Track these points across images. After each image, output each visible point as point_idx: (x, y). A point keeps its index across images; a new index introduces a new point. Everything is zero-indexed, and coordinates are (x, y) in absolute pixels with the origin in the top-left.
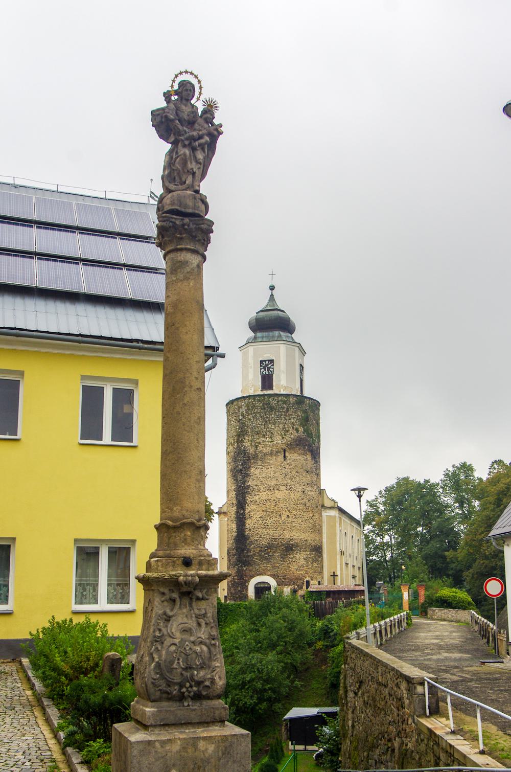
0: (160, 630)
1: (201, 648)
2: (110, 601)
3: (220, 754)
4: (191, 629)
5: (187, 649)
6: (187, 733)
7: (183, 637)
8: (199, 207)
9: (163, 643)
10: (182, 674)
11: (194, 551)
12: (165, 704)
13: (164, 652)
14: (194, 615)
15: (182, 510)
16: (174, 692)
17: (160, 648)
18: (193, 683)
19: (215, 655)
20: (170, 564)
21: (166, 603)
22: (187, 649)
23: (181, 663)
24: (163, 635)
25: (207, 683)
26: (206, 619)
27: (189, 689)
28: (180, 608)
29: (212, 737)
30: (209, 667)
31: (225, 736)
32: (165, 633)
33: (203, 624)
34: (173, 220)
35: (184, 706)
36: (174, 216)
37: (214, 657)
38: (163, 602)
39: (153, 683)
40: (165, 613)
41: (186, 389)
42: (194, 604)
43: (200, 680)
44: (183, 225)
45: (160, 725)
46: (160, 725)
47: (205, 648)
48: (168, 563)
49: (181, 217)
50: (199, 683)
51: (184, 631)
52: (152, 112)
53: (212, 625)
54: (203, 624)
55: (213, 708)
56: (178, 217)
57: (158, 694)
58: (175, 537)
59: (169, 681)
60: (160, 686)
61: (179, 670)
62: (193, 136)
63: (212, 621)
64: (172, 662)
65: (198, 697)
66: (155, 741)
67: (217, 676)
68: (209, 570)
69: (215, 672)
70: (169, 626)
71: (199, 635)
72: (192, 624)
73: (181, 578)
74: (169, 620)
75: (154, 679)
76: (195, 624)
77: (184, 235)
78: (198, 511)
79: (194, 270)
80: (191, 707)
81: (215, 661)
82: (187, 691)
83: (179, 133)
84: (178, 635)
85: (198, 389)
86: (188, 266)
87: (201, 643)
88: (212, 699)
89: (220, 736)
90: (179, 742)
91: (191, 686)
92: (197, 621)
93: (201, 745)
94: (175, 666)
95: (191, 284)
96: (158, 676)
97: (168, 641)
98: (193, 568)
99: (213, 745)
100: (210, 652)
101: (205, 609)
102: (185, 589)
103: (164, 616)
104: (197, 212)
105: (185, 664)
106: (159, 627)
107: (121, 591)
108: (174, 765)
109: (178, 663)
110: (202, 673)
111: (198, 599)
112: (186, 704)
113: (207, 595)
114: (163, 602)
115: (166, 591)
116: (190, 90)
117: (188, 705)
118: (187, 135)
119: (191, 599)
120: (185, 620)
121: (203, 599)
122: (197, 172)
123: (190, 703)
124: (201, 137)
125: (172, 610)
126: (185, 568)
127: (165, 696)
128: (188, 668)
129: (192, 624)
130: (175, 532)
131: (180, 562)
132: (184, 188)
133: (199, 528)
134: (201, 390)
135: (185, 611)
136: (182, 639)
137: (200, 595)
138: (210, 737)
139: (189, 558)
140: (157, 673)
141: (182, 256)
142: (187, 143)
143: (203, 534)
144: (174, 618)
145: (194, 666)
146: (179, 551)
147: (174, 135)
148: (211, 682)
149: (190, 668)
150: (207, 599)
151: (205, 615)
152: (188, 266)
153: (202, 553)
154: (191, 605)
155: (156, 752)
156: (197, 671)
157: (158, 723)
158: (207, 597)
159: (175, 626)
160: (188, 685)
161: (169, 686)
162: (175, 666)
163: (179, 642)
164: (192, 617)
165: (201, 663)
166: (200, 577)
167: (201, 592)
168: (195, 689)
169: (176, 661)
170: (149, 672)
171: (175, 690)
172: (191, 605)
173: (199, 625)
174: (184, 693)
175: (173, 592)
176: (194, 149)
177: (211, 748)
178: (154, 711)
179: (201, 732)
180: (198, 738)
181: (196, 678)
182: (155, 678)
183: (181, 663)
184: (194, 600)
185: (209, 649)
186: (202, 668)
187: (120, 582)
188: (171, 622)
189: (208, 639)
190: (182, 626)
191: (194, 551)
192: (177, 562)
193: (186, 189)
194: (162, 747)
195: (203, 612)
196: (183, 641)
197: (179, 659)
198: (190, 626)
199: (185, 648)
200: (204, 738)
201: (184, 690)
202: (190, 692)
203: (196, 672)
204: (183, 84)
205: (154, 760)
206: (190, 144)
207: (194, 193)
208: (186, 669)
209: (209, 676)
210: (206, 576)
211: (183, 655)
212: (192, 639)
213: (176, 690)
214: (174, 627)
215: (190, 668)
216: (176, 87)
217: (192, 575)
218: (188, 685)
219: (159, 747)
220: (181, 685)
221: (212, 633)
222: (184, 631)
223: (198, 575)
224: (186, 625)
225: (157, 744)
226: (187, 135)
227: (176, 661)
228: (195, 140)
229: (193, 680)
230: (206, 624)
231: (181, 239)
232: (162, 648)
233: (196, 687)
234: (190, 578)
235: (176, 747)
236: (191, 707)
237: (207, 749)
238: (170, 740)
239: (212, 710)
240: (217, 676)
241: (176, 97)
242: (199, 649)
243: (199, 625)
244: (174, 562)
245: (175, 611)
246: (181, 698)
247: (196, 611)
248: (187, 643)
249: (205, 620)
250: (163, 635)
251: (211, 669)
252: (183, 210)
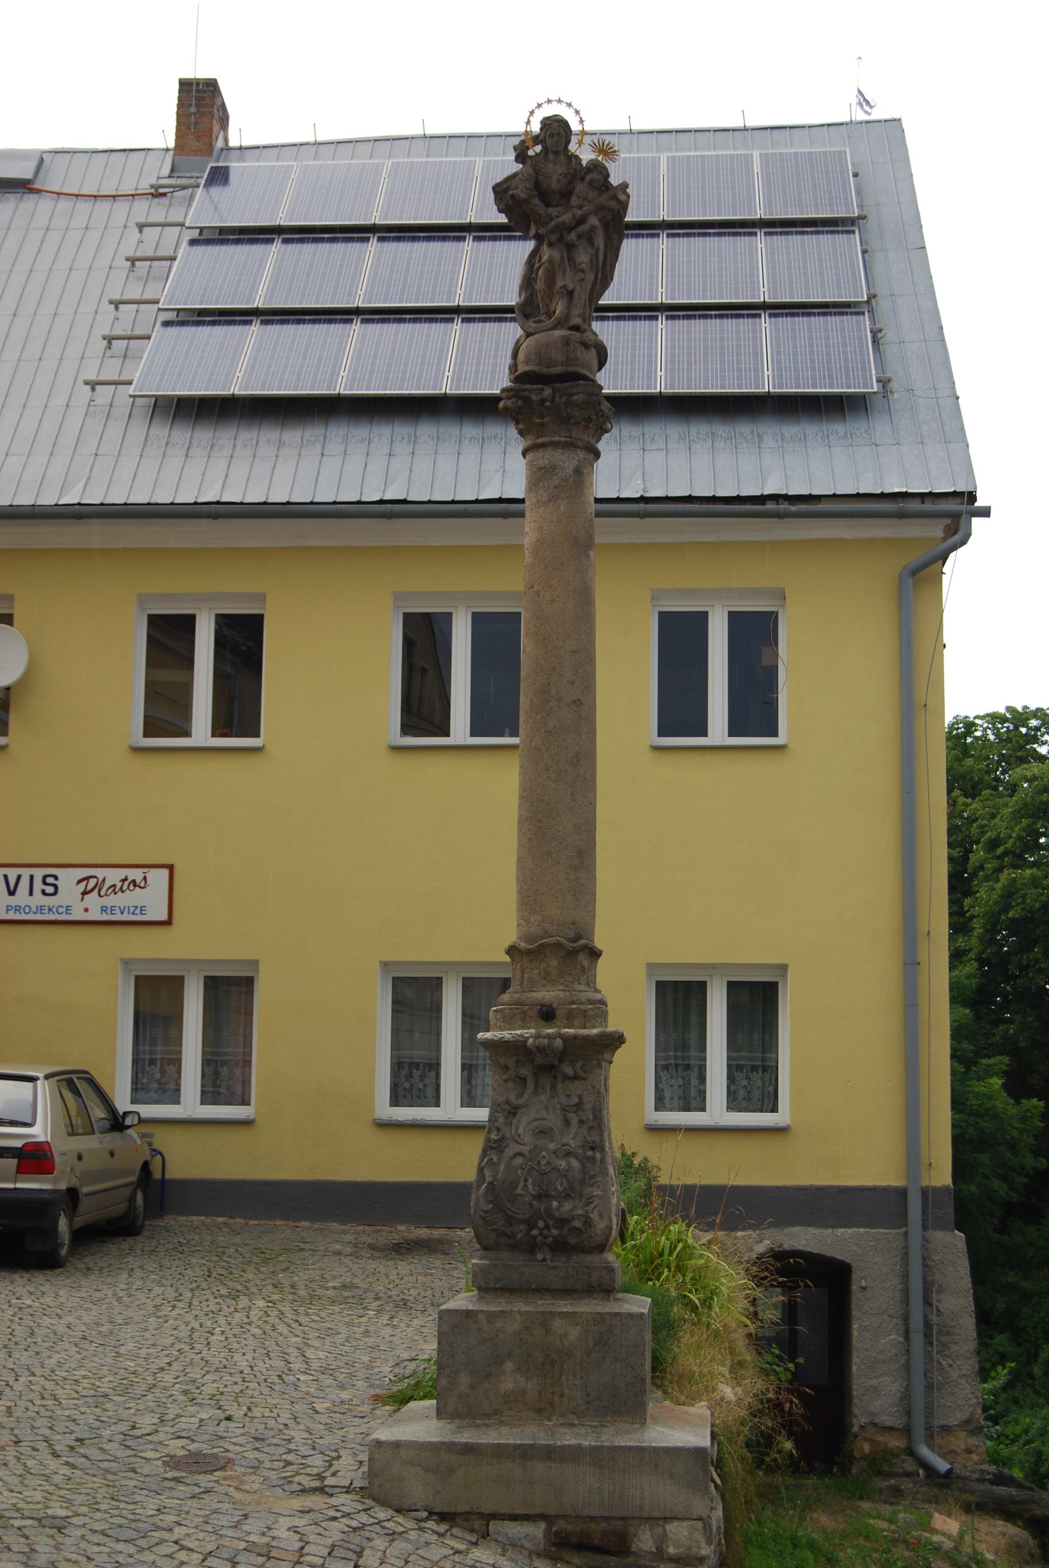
0: (498, 1129)
1: (568, 1164)
2: (734, 1103)
3: (591, 1342)
4: (551, 1129)
5: (543, 1163)
6: (542, 1305)
7: (538, 1143)
8: (576, 359)
9: (502, 1152)
10: (531, 1205)
11: (562, 994)
12: (504, 1254)
13: (502, 1167)
14: (558, 1106)
15: (543, 921)
16: (519, 1236)
17: (495, 1159)
18: (551, 1222)
19: (594, 1176)
20: (518, 1016)
21: (510, 1085)
22: (543, 1163)
23: (530, 1187)
24: (503, 1138)
25: (577, 1224)
26: (580, 1112)
27: (545, 1232)
28: (535, 1093)
29: (576, 1313)
30: (581, 1197)
31: (600, 1314)
32: (508, 1135)
33: (574, 1122)
34: (526, 393)
35: (536, 1260)
36: (528, 386)
37: (590, 1180)
38: (506, 1081)
39: (483, 1218)
40: (507, 1102)
41: (551, 704)
42: (559, 1086)
43: (563, 1217)
44: (543, 401)
45: (496, 1289)
46: (496, 1289)
47: (575, 1163)
48: (515, 1015)
49: (539, 386)
50: (562, 1223)
51: (540, 1132)
52: (494, 188)
53: (591, 1124)
54: (574, 1122)
55: (588, 1268)
56: (535, 387)
57: (492, 1236)
58: (532, 969)
59: (511, 1217)
60: (494, 1223)
61: (528, 1199)
62: (563, 223)
63: (591, 1117)
64: (514, 1185)
65: (561, 1247)
66: (477, 1312)
67: (596, 1213)
68: (585, 1028)
69: (592, 1206)
70: (515, 1122)
71: (565, 1140)
72: (554, 1121)
73: (531, 1040)
74: (515, 1114)
75: (485, 1212)
76: (559, 1122)
77: (546, 419)
78: (574, 923)
79: (567, 481)
80: (549, 1262)
81: (592, 1185)
82: (541, 1234)
83: (541, 222)
84: (528, 1138)
85: (574, 702)
86: (556, 474)
87: (568, 1154)
88: (589, 1253)
89: (590, 1313)
90: (518, 1316)
91: (547, 1227)
92: (565, 1115)
93: (557, 1324)
94: (519, 1191)
95: (562, 508)
96: (491, 1206)
97: (512, 1149)
98: (558, 1023)
99: (578, 1328)
100: (584, 1170)
101: (580, 1097)
102: (539, 1060)
103: (506, 1106)
104: (571, 369)
105: (537, 1189)
106: (496, 1124)
107: (744, 1082)
108: (509, 1355)
109: (526, 1186)
110: (567, 1206)
111: (566, 1078)
112: (540, 1257)
113: (585, 1072)
114: (506, 1081)
115: (511, 1063)
116: (558, 134)
117: (544, 1260)
118: (553, 223)
119: (555, 1077)
120: (543, 1114)
121: (575, 1078)
122: (577, 288)
123: (548, 1256)
124: (581, 221)
125: (520, 1096)
126: (543, 1023)
127: (504, 1240)
128: (543, 1196)
129: (554, 1120)
130: (531, 961)
131: (534, 1013)
132: (550, 326)
133: (573, 953)
134: (581, 703)
135: (542, 1098)
136: (536, 1146)
137: (569, 1071)
138: (572, 1313)
139: (551, 1006)
140: (491, 1202)
141: (546, 456)
142: (554, 238)
143: (586, 963)
144: (524, 1110)
145: (553, 1193)
146: (535, 994)
147: (535, 223)
148: (585, 1222)
149: (547, 1196)
150: (584, 1079)
151: (579, 1106)
152: (556, 474)
153: (575, 998)
154: (553, 1087)
155: (479, 1329)
156: (559, 1202)
157: (491, 1285)
158: (583, 1075)
159: (523, 1123)
160: (541, 1224)
161: (511, 1225)
162: (519, 1191)
163: (530, 1151)
164: (554, 1108)
165: (565, 1189)
166: (566, 1039)
167: (573, 1066)
168: (554, 1232)
169: (522, 1184)
170: (477, 1199)
171: (520, 1232)
172: (553, 1087)
173: (567, 1123)
174: (535, 1237)
175: (523, 1065)
176: (570, 247)
177: (575, 1333)
178: (485, 1265)
179: (564, 1306)
180: (552, 1314)
181: (556, 1214)
182: (485, 1209)
183: (530, 1187)
184: (560, 1079)
185: (583, 1165)
186: (568, 1197)
187: (743, 1062)
188: (518, 1116)
189: (582, 1146)
190: (537, 1123)
191: (562, 994)
192: (530, 1013)
193: (554, 328)
194: (489, 1322)
195: (576, 1100)
196: (536, 1150)
197: (526, 1180)
198: (550, 1124)
199: (539, 1162)
200: (563, 1315)
201: (535, 1232)
202: (546, 1237)
203: (555, 1204)
204: (547, 123)
205: (476, 1343)
206: (561, 239)
207: (569, 332)
208: (539, 1197)
209: (580, 1212)
210: (575, 1037)
211: (535, 1173)
212: (552, 1146)
213: (521, 1231)
214: (523, 1125)
215: (547, 1196)
216: (536, 127)
217: (549, 1036)
218: (541, 1224)
219: (485, 1322)
220: (531, 1225)
221: (589, 1138)
222: (540, 1132)
223: (561, 1036)
224: (543, 1122)
225: (482, 1318)
226: (553, 223)
227: (522, 1184)
228: (570, 229)
229: (551, 1217)
230: (581, 1122)
231: (542, 425)
232: (499, 1159)
233: (557, 1228)
234: (546, 1041)
235: (514, 1325)
236: (549, 1262)
237: (566, 1334)
238: (503, 1312)
239: (586, 1271)
240: (596, 1213)
241: (538, 148)
242: (564, 1164)
243: (567, 1123)
244: (524, 1013)
245: (525, 1097)
246: (532, 1247)
247: (563, 1099)
248: (544, 1153)
249: (578, 1115)
250: (503, 1138)
251: (584, 1199)
252: (545, 370)
